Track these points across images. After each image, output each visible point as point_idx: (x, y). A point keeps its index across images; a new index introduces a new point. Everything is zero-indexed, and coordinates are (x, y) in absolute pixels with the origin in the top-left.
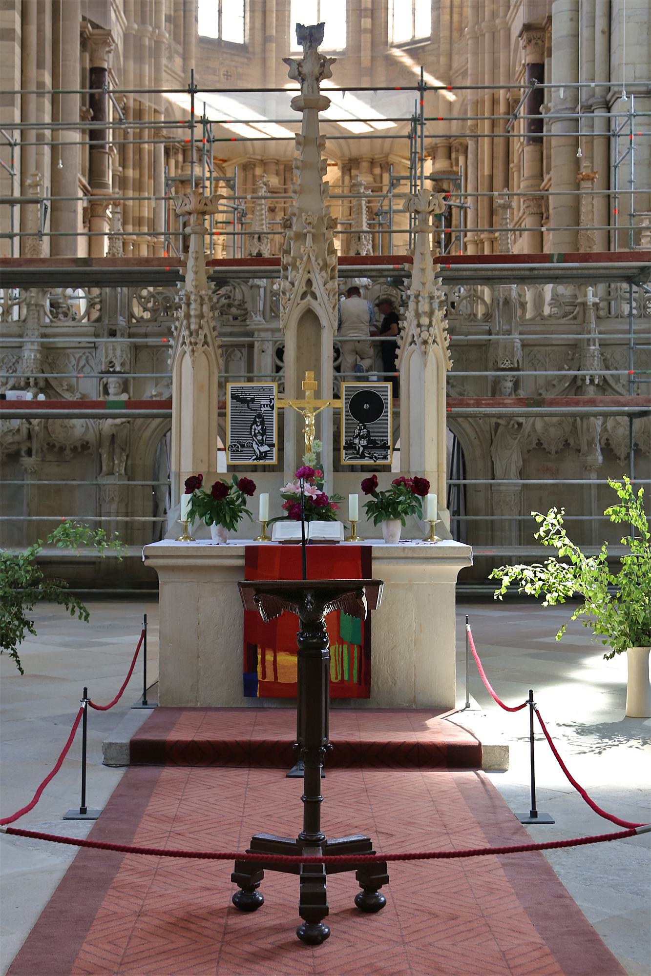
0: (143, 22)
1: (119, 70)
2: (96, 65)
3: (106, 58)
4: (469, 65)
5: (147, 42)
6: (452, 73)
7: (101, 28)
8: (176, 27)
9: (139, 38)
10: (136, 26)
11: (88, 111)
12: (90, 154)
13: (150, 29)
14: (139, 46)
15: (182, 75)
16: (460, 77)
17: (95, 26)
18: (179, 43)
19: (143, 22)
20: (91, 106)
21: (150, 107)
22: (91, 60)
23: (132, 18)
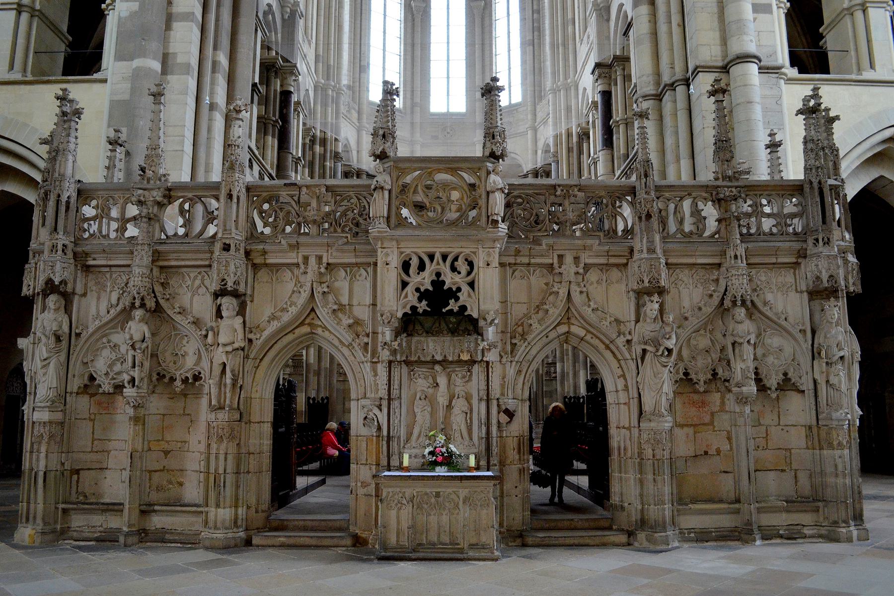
0: (328, 79)
1: (310, 109)
2: (285, 89)
3: (292, 84)
4: (551, 115)
5: (330, 92)
6: (536, 124)
7: (290, 62)
8: (353, 93)
9: (324, 89)
10: (323, 81)
11: (277, 121)
12: (278, 153)
13: (333, 84)
14: (325, 96)
15: (358, 124)
16: (542, 126)
17: (286, 60)
18: (355, 103)
19: (328, 79)
20: (280, 117)
21: (332, 137)
22: (281, 86)
23: (321, 76)
